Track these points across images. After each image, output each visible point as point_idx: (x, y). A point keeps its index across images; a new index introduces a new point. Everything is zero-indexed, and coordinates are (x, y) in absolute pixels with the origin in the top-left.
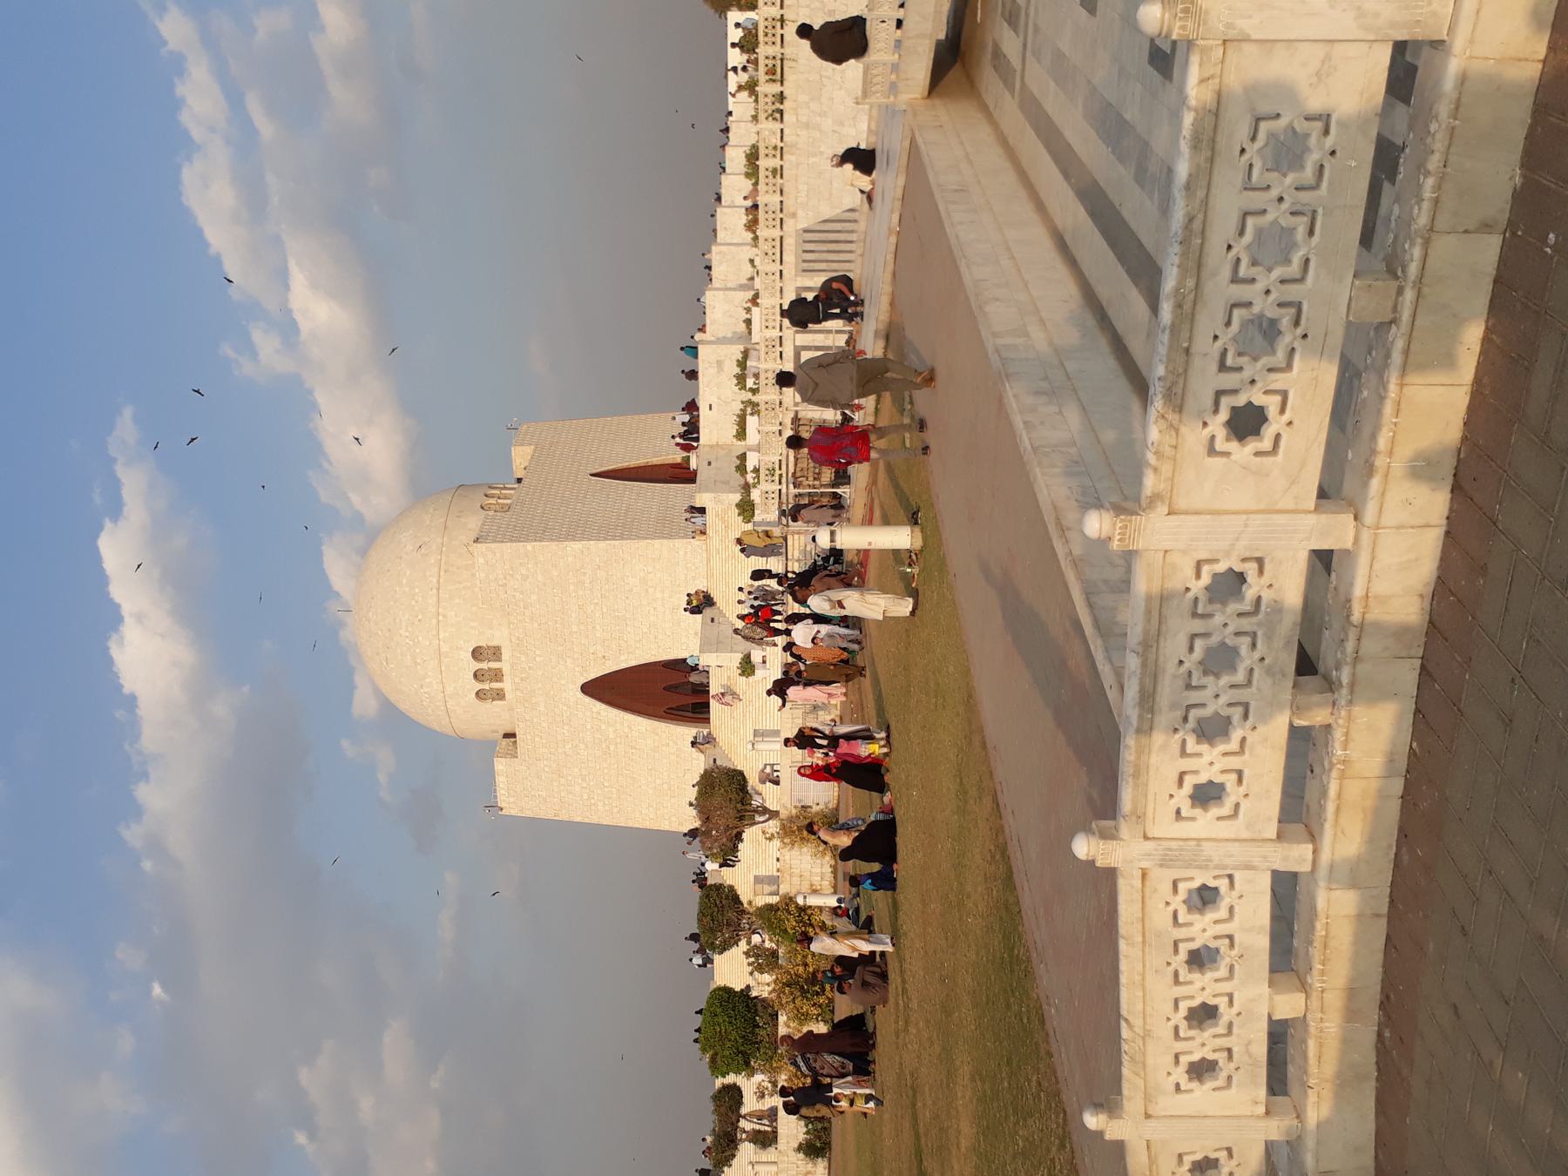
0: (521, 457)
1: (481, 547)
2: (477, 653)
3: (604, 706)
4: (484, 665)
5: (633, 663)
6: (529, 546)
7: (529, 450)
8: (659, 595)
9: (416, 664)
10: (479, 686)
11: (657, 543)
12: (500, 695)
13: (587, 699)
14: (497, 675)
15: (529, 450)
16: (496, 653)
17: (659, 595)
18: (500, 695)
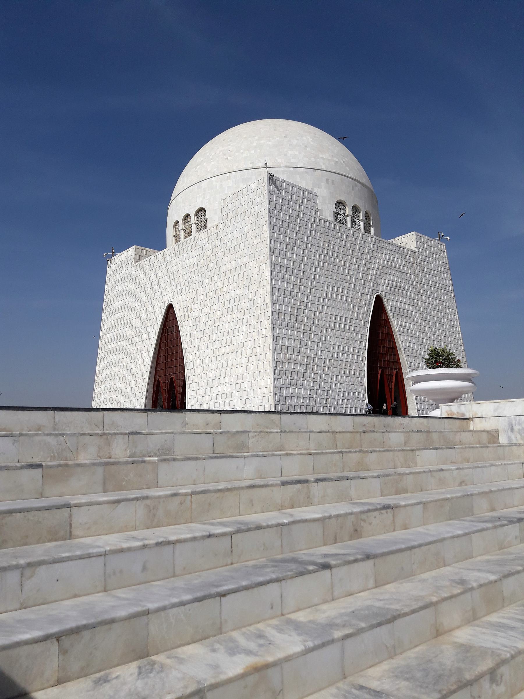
0: (409, 240)
1: (266, 179)
2: (201, 211)
3: (159, 325)
4: (193, 220)
5: (184, 346)
6: (266, 229)
7: (413, 246)
8: (230, 364)
9: (196, 167)
10: (180, 222)
11: (270, 355)
12: (177, 240)
13: (163, 311)
14: (188, 233)
15: (413, 246)
16: (202, 226)
17: (230, 364)
18: (177, 240)
